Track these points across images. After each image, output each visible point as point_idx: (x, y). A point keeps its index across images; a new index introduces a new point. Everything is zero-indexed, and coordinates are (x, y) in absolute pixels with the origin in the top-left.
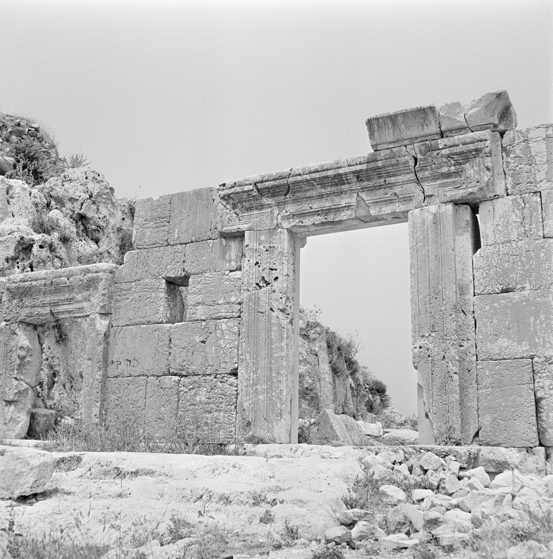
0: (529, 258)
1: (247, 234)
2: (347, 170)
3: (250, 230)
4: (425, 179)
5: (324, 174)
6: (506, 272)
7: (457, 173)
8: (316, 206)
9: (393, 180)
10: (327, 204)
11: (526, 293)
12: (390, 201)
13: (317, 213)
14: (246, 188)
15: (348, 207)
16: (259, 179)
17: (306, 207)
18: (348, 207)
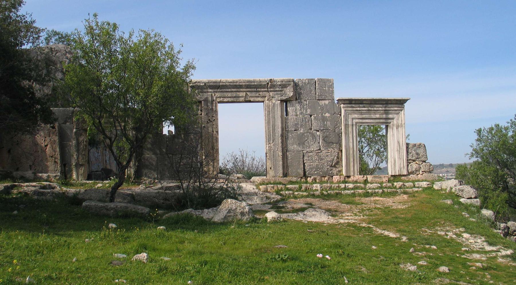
0: (303, 121)
1: (203, 102)
2: (244, 84)
3: (204, 100)
4: (271, 91)
5: (235, 84)
6: (296, 125)
7: (281, 91)
8: (229, 95)
9: (260, 90)
10: (234, 94)
11: (301, 131)
12: (258, 97)
13: (230, 97)
14: (202, 84)
15: (242, 97)
16: (207, 81)
17: (226, 94)
18: (242, 97)
